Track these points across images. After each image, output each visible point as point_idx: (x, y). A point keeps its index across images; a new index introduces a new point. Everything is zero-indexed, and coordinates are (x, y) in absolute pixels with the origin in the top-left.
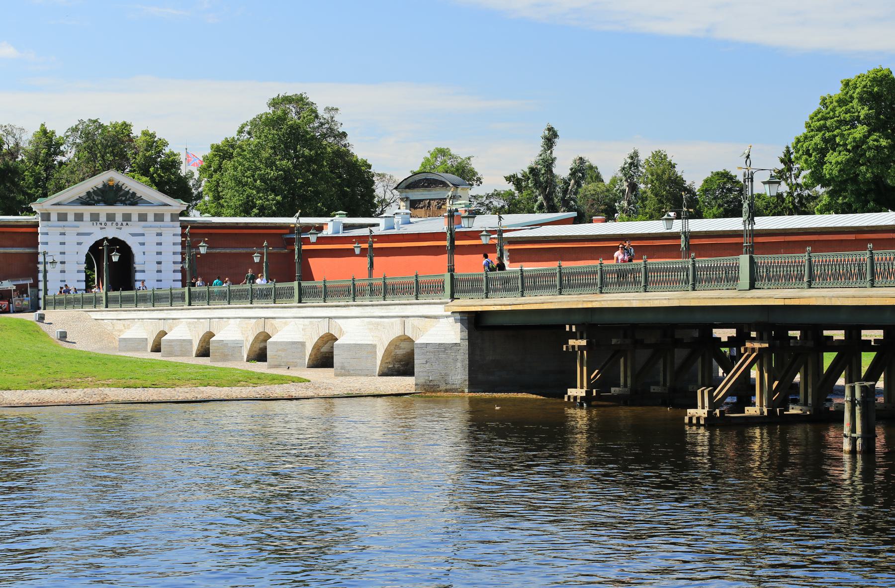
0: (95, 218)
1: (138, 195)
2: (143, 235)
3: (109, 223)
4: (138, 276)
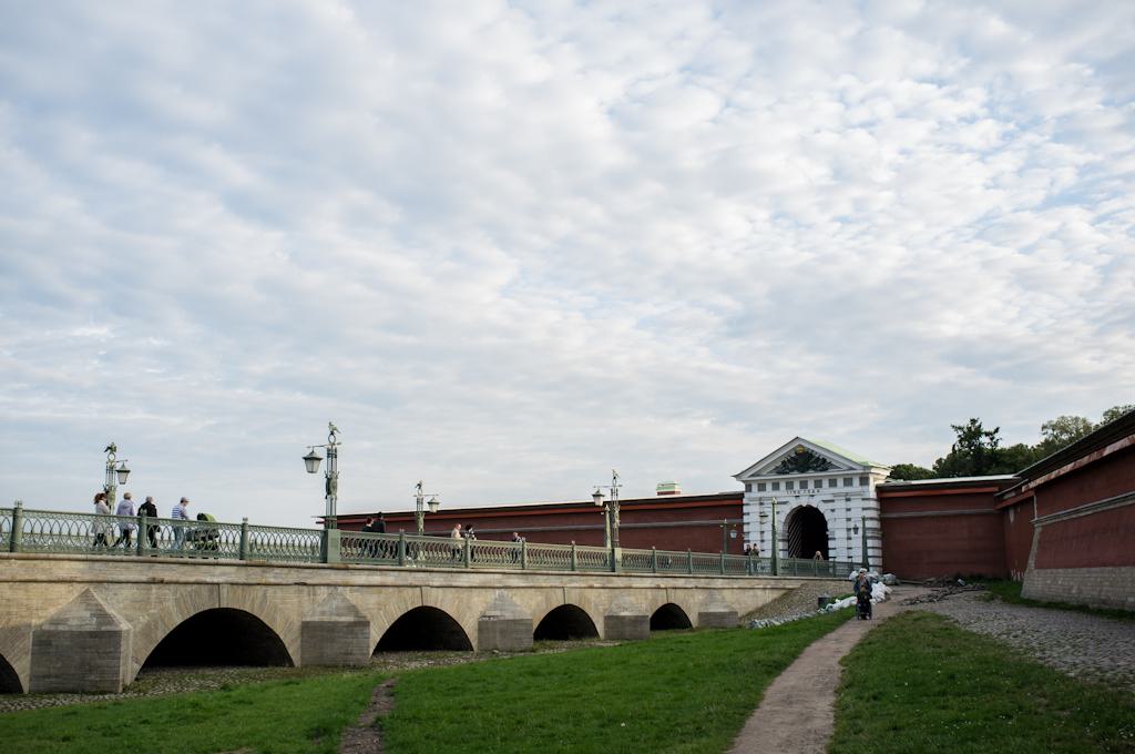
0: (790, 485)
1: (828, 461)
2: (833, 501)
3: (802, 492)
4: (831, 544)
